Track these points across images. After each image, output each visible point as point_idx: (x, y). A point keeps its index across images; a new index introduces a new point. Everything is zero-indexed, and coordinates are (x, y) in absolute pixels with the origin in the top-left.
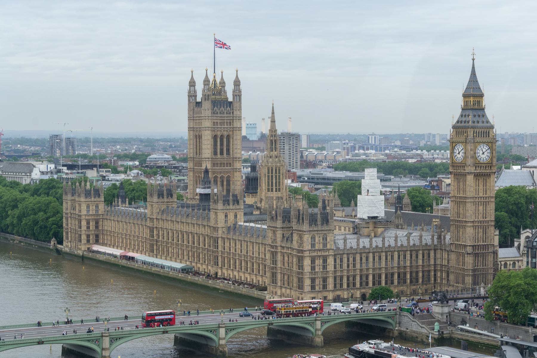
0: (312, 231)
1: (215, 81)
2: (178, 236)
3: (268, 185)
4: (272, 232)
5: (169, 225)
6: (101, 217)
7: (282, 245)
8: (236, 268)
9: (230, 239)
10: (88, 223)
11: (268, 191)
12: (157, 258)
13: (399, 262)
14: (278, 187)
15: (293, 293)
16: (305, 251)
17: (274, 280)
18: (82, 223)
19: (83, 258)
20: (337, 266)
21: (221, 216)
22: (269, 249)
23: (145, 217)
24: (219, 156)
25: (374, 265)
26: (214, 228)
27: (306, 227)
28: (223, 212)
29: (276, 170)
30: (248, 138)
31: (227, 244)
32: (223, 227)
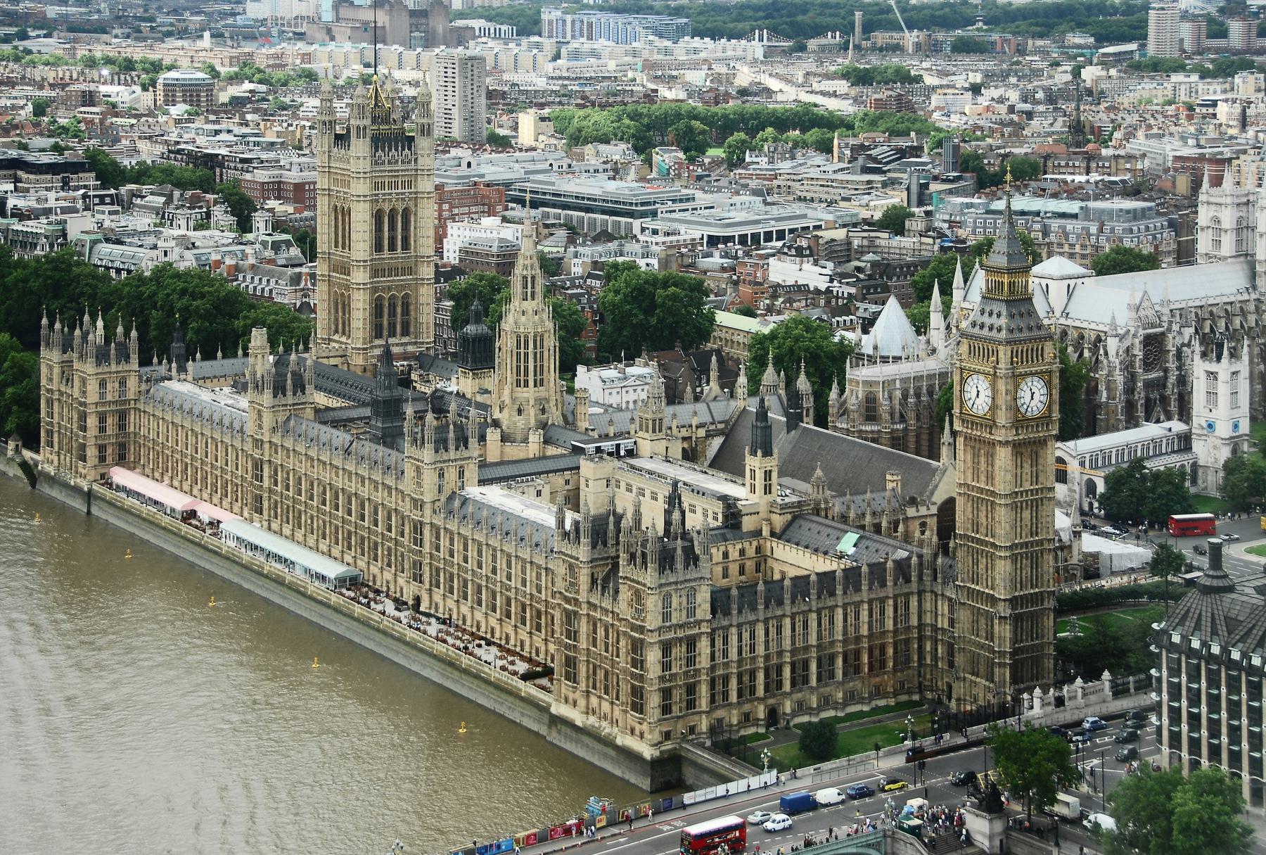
3: (518, 373)
4: (566, 565)
9: (452, 533)
10: (102, 418)
11: (518, 385)
13: (845, 627)
14: (539, 377)
17: (572, 677)
18: (88, 420)
20: (717, 654)
21: (429, 478)
23: (242, 431)
24: (386, 254)
25: (793, 643)
26: (415, 501)
27: (649, 577)
31: (445, 542)
32: (434, 502)
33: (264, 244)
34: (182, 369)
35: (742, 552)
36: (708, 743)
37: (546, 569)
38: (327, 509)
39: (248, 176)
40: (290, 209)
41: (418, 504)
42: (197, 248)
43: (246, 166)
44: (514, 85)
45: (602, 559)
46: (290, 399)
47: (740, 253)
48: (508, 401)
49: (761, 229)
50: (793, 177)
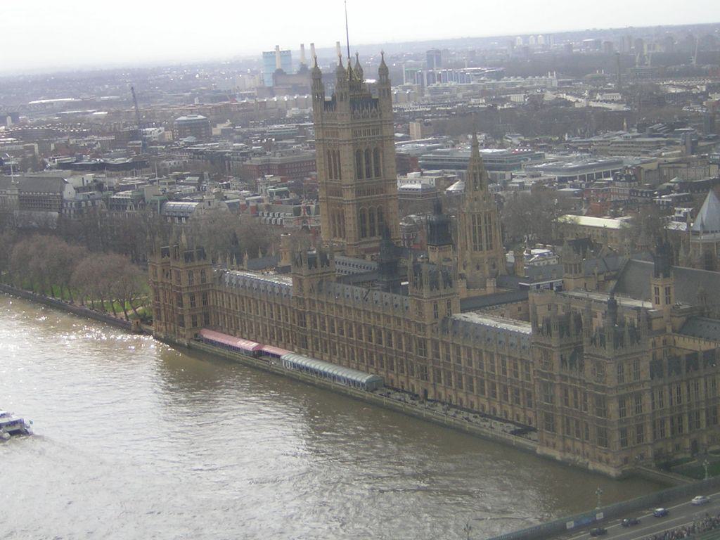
0: (619, 356)
1: (351, 69)
2: (351, 328)
5: (332, 310)
6: (210, 288)
7: (563, 373)
8: (462, 388)
9: (446, 344)
10: (192, 298)
12: (313, 357)
15: (588, 448)
16: (609, 389)
18: (184, 299)
19: (189, 347)
21: (428, 309)
22: (538, 377)
24: (365, 180)
25: (706, 396)
26: (418, 325)
27: (608, 352)
28: (431, 302)
29: (485, 218)
30: (285, 71)
31: (442, 351)
33: (271, 193)
34: (240, 262)
35: (654, 344)
36: (654, 465)
37: (521, 360)
38: (354, 339)
39: (248, 162)
40: (278, 179)
41: (421, 327)
42: (229, 199)
43: (244, 157)
44: (400, 109)
45: (567, 345)
46: (320, 270)
47: (584, 185)
48: (469, 261)
49: (594, 171)
50: (604, 143)
